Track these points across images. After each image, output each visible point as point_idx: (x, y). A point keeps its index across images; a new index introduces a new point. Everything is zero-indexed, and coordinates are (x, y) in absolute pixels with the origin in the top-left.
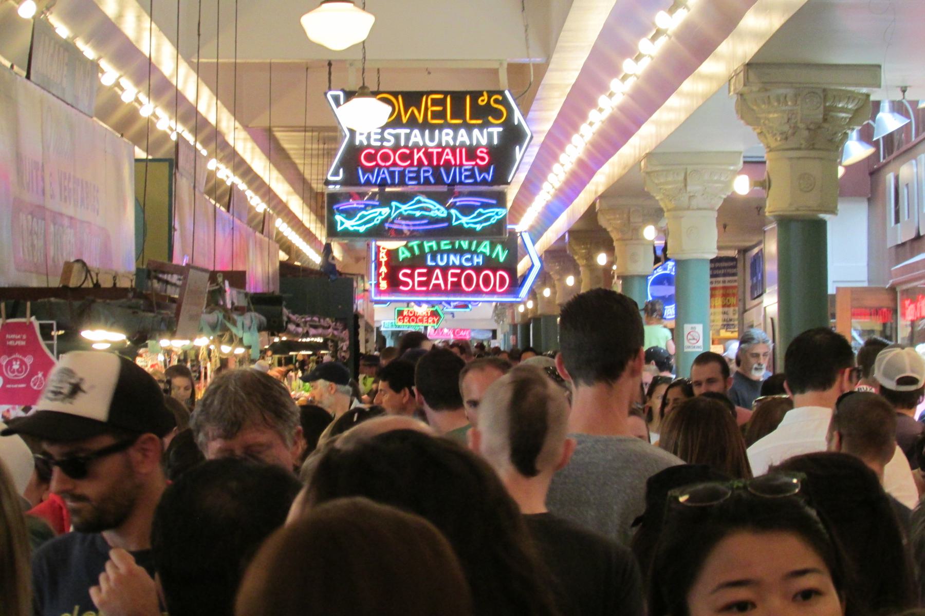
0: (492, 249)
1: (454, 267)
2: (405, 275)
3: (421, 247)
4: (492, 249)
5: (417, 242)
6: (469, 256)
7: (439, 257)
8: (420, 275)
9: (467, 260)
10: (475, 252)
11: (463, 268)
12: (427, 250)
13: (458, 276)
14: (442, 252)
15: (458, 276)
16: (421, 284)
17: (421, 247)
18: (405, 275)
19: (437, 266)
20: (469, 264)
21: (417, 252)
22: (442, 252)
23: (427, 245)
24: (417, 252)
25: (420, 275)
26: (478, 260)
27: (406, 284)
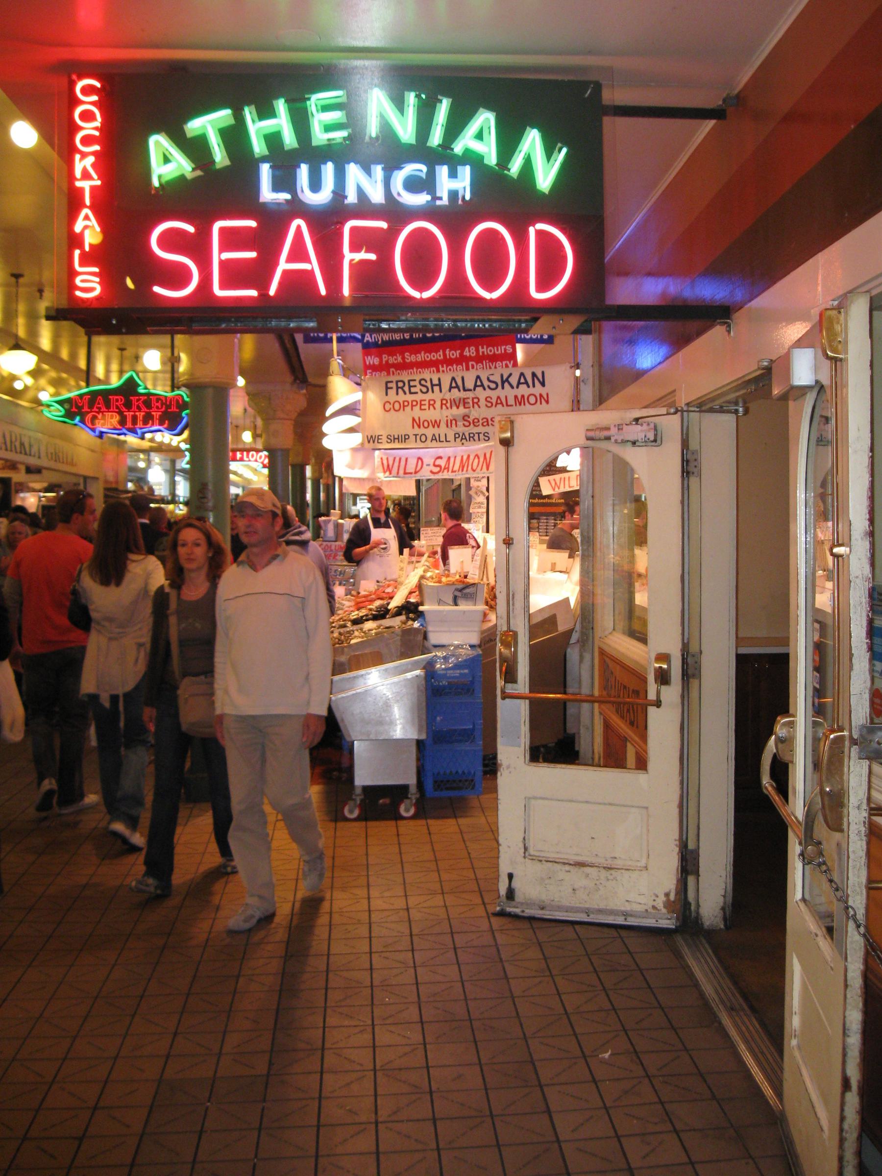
0: (508, 142)
1: (364, 209)
2: (171, 241)
3: (234, 137)
4: (508, 142)
5: (223, 116)
6: (418, 168)
7: (303, 171)
8: (231, 240)
9: (413, 185)
10: (442, 156)
11: (397, 214)
12: (259, 147)
13: (381, 243)
14: (316, 157)
15: (381, 243)
16: (233, 274)
17: (234, 137)
18: (171, 241)
19: (297, 208)
20: (420, 199)
21: (220, 156)
22: (316, 157)
23: (257, 130)
24: (220, 156)
25: (231, 240)
26: (454, 184)
27: (179, 277)
